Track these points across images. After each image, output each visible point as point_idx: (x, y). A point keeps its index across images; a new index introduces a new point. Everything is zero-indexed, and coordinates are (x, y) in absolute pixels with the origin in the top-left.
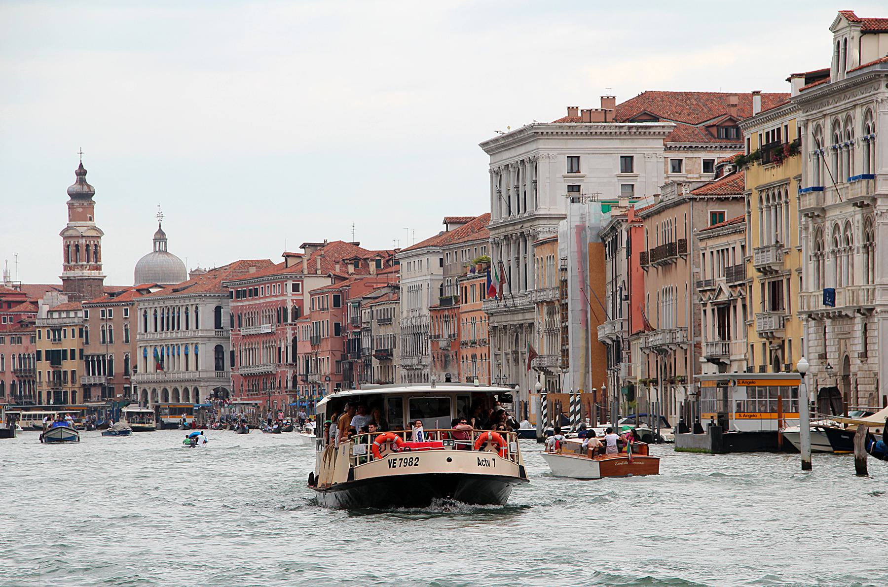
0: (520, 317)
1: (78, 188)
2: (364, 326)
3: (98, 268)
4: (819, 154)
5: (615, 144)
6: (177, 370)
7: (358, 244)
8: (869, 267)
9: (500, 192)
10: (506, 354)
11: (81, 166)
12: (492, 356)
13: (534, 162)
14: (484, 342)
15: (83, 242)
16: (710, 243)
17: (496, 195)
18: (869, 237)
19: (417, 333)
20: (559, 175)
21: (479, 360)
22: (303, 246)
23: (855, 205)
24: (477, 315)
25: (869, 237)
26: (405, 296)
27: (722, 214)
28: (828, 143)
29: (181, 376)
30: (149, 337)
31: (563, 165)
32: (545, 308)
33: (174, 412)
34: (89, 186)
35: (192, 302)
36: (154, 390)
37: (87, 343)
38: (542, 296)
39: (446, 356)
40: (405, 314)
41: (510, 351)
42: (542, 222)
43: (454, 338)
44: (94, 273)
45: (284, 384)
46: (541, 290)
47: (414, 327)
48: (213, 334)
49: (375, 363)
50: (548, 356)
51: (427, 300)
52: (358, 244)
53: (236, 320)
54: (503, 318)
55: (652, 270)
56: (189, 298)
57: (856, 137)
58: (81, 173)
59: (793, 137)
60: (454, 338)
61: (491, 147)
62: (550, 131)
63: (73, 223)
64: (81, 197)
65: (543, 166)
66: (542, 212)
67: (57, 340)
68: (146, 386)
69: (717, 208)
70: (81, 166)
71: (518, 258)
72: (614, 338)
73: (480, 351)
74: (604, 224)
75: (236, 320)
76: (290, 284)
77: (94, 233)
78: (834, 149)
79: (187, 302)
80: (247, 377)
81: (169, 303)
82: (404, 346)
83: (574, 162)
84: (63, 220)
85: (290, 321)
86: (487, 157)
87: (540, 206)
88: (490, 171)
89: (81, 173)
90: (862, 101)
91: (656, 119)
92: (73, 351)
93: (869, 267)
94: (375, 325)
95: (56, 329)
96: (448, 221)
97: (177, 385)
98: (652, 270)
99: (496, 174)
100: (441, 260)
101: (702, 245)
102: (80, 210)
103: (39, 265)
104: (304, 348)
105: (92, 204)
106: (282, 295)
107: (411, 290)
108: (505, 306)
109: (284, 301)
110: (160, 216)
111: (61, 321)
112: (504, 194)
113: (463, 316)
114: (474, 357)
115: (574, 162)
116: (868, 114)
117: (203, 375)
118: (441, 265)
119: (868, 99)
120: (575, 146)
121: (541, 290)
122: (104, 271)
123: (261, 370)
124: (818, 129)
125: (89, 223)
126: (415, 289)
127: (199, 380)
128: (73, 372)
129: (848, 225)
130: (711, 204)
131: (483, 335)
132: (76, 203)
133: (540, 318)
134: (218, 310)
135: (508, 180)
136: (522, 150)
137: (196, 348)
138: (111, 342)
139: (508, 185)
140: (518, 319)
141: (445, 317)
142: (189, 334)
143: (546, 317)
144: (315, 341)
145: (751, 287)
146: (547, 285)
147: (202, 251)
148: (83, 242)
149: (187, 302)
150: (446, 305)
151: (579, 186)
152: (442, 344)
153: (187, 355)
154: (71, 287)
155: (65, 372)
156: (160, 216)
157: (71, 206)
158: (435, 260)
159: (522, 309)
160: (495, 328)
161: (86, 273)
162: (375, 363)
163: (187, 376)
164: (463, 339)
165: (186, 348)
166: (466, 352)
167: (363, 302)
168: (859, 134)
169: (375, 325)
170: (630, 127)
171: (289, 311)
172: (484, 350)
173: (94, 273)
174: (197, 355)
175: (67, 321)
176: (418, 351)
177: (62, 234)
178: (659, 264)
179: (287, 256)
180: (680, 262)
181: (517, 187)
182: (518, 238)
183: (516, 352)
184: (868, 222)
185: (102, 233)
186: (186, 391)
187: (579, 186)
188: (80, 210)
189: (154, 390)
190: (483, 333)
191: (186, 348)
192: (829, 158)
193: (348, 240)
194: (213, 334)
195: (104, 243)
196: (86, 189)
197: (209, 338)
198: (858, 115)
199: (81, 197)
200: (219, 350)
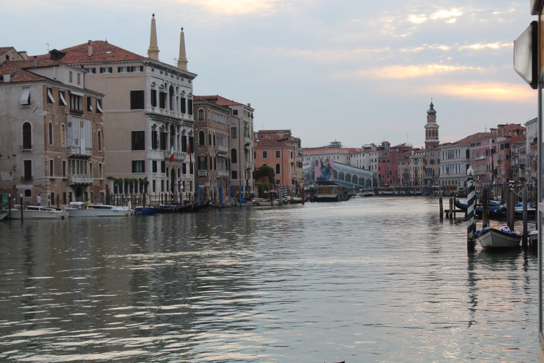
1: (430, 111)
3: (437, 139)
7: (520, 125)
22: (499, 126)
30: (444, 161)
44: (436, 140)
49: (520, 170)
52: (520, 125)
56: (457, 147)
58: (432, 106)
64: (432, 114)
76: (491, 140)
77: (436, 126)
81: (451, 149)
89: (432, 106)
94: (520, 155)
105: (435, 117)
109: (489, 147)
117: (462, 175)
122: (440, 140)
127: (460, 177)
134: (468, 152)
157: (428, 117)
162: (520, 170)
163: (456, 176)
169: (520, 155)
173: (436, 140)
177: (425, 127)
179: (492, 129)
197: (464, 162)
199: (432, 114)
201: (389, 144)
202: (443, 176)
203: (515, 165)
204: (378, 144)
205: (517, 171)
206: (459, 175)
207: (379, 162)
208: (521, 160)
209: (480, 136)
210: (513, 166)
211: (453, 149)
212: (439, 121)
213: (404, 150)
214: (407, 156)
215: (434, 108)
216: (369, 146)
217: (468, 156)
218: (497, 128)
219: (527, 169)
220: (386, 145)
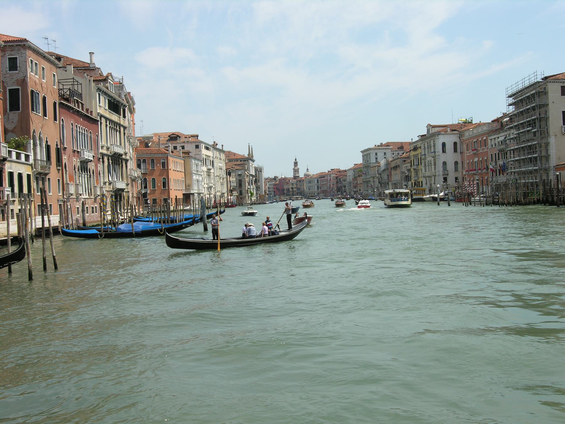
4: (425, 149)
8: (435, 168)
13: (370, 154)
18: (435, 163)
19: (350, 183)
25: (435, 163)
28: (426, 147)
51: (351, 178)
59: (419, 146)
60: (357, 183)
64: (296, 164)
93: (435, 168)
104: (331, 186)
124: (424, 145)
135: (365, 157)
144: (333, 185)
147: (314, 171)
150: (355, 178)
154: (295, 177)
176: (350, 186)
184: (435, 160)
192: (427, 149)
199: (296, 164)
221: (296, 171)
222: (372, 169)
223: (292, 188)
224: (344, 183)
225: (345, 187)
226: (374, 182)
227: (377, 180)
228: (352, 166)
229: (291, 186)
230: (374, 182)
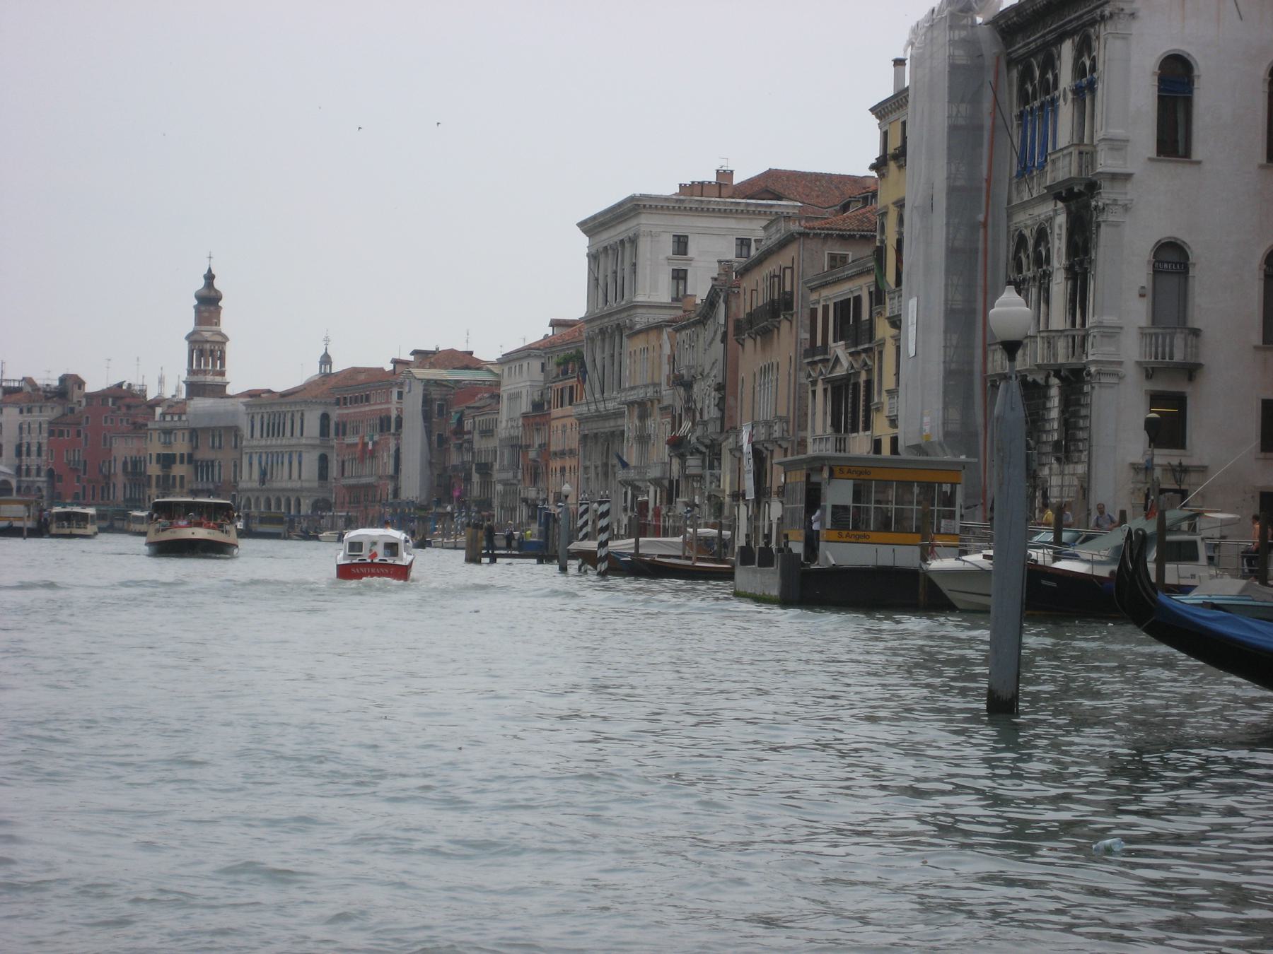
0: (612, 423)
1: (206, 292)
2: (466, 437)
3: (222, 374)
5: (731, 223)
6: (282, 480)
7: (471, 353)
9: (597, 280)
10: (596, 467)
11: (210, 270)
12: (581, 469)
13: (634, 241)
14: (572, 453)
15: (208, 346)
16: (825, 293)
17: (592, 281)
20: (662, 257)
21: (567, 474)
22: (412, 354)
23: (1058, 197)
24: (568, 421)
26: (504, 405)
27: (845, 257)
29: (284, 485)
30: (255, 443)
31: (668, 246)
32: (636, 412)
33: (263, 521)
34: (217, 291)
35: (298, 408)
36: (258, 498)
37: (197, 447)
38: (632, 396)
39: (536, 468)
40: (504, 424)
41: (599, 463)
42: (640, 311)
43: (544, 447)
44: (218, 379)
45: (384, 497)
46: (632, 388)
47: (512, 438)
48: (318, 442)
49: (476, 478)
50: (635, 467)
52: (471, 353)
53: (342, 429)
54: (594, 426)
55: (749, 343)
56: (295, 403)
57: (1061, 87)
58: (210, 277)
61: (591, 227)
62: (654, 204)
63: (199, 328)
64: (209, 302)
65: (644, 245)
66: (640, 298)
67: (168, 444)
68: (249, 494)
69: (838, 251)
70: (210, 270)
71: (613, 356)
72: (707, 441)
73: (569, 462)
74: (643, 216)
75: (342, 429)
76: (395, 391)
77: (219, 338)
78: (1021, 116)
79: (293, 408)
80: (350, 488)
81: (276, 409)
82: (502, 460)
83: (681, 244)
84: (189, 325)
85: (393, 430)
86: (584, 240)
87: (639, 291)
88: (588, 255)
89: (210, 277)
90: (1074, 24)
91: (780, 199)
92: (182, 455)
94: (476, 436)
95: (168, 432)
96: (555, 324)
97: (249, 494)
98: (749, 343)
99: (593, 258)
100: (543, 364)
101: (814, 297)
102: (206, 314)
103: (162, 371)
105: (218, 309)
106: (387, 402)
107: (510, 398)
108: (597, 410)
109: (388, 410)
110: (327, 340)
111: (172, 424)
112: (601, 282)
113: (554, 423)
114: (563, 469)
115: (681, 244)
116: (1085, 47)
117: (306, 485)
118: (543, 370)
119: (1086, 18)
120: (684, 224)
121: (632, 388)
122: (228, 377)
123: (364, 481)
125: (214, 328)
126: (515, 397)
127: (301, 490)
128: (182, 477)
129: (1042, 235)
130: (830, 243)
131: (574, 443)
132: (203, 308)
133: (630, 425)
134: (325, 418)
136: (622, 227)
137: (300, 456)
138: (220, 447)
139: (606, 270)
140: (609, 425)
141: (537, 424)
142: (294, 441)
143: (637, 422)
145: (881, 353)
146: (639, 382)
148: (208, 346)
149: (293, 408)
150: (539, 413)
151: (686, 271)
152: (532, 454)
153: (290, 463)
155: (174, 477)
156: (327, 340)
157: (197, 309)
158: (536, 365)
159: (614, 414)
160: (585, 437)
161: (209, 378)
162: (476, 478)
163: (290, 485)
164: (553, 448)
165: (290, 456)
166: (556, 464)
167: (467, 412)
168: (1066, 78)
169: (476, 436)
170: (748, 204)
171: (393, 420)
172: (573, 462)
173: (218, 379)
174: (300, 463)
175: (178, 424)
177: (188, 337)
178: (757, 333)
179: (396, 362)
180: (785, 326)
181: (615, 272)
182: (613, 332)
183: (606, 465)
185: (227, 339)
186: (288, 501)
187: (686, 271)
188: (206, 314)
189: (258, 498)
190: (573, 441)
191: (290, 456)
193: (461, 348)
194: (318, 442)
195: (230, 349)
196: (213, 293)
197: (314, 446)
198: (1067, 50)
199: (209, 302)
200: (324, 460)
201: (80, 383)
202: (249, 485)
203: (463, 463)
204: (48, 376)
205: (468, 479)
206: (298, 485)
207: (51, 433)
208: (480, 451)
209: (362, 377)
210: (455, 467)
211: (284, 409)
212: (228, 322)
213: (124, 403)
214: (140, 421)
215: (217, 284)
216: (16, 384)
217: (324, 431)
218: (412, 358)
219: (497, 475)
220: (70, 383)
221: (207, 349)
222: (639, 343)
223: (167, 461)
224: (479, 443)
225: (485, 469)
226: (643, 439)
227: (659, 427)
228: (538, 331)
229: (155, 447)
230: (643, 439)
